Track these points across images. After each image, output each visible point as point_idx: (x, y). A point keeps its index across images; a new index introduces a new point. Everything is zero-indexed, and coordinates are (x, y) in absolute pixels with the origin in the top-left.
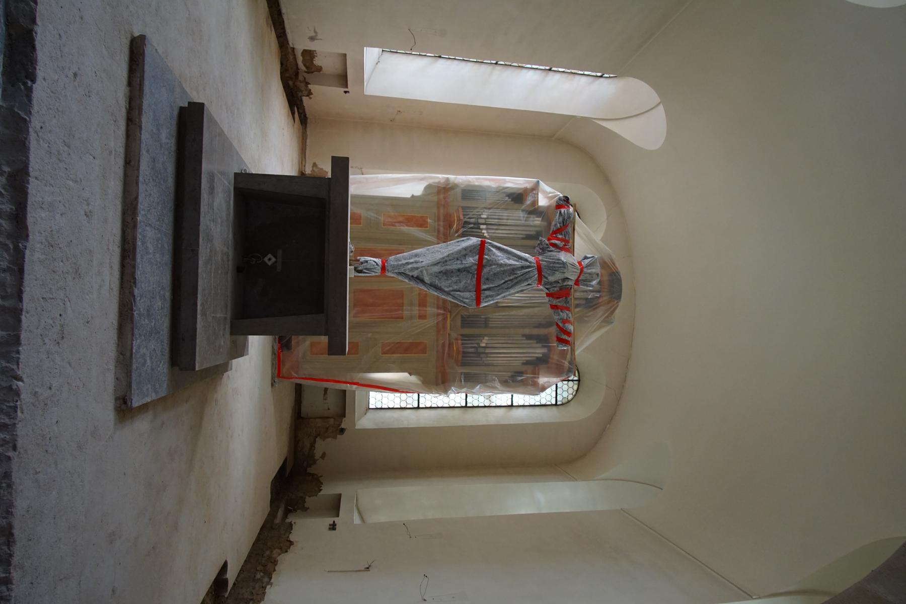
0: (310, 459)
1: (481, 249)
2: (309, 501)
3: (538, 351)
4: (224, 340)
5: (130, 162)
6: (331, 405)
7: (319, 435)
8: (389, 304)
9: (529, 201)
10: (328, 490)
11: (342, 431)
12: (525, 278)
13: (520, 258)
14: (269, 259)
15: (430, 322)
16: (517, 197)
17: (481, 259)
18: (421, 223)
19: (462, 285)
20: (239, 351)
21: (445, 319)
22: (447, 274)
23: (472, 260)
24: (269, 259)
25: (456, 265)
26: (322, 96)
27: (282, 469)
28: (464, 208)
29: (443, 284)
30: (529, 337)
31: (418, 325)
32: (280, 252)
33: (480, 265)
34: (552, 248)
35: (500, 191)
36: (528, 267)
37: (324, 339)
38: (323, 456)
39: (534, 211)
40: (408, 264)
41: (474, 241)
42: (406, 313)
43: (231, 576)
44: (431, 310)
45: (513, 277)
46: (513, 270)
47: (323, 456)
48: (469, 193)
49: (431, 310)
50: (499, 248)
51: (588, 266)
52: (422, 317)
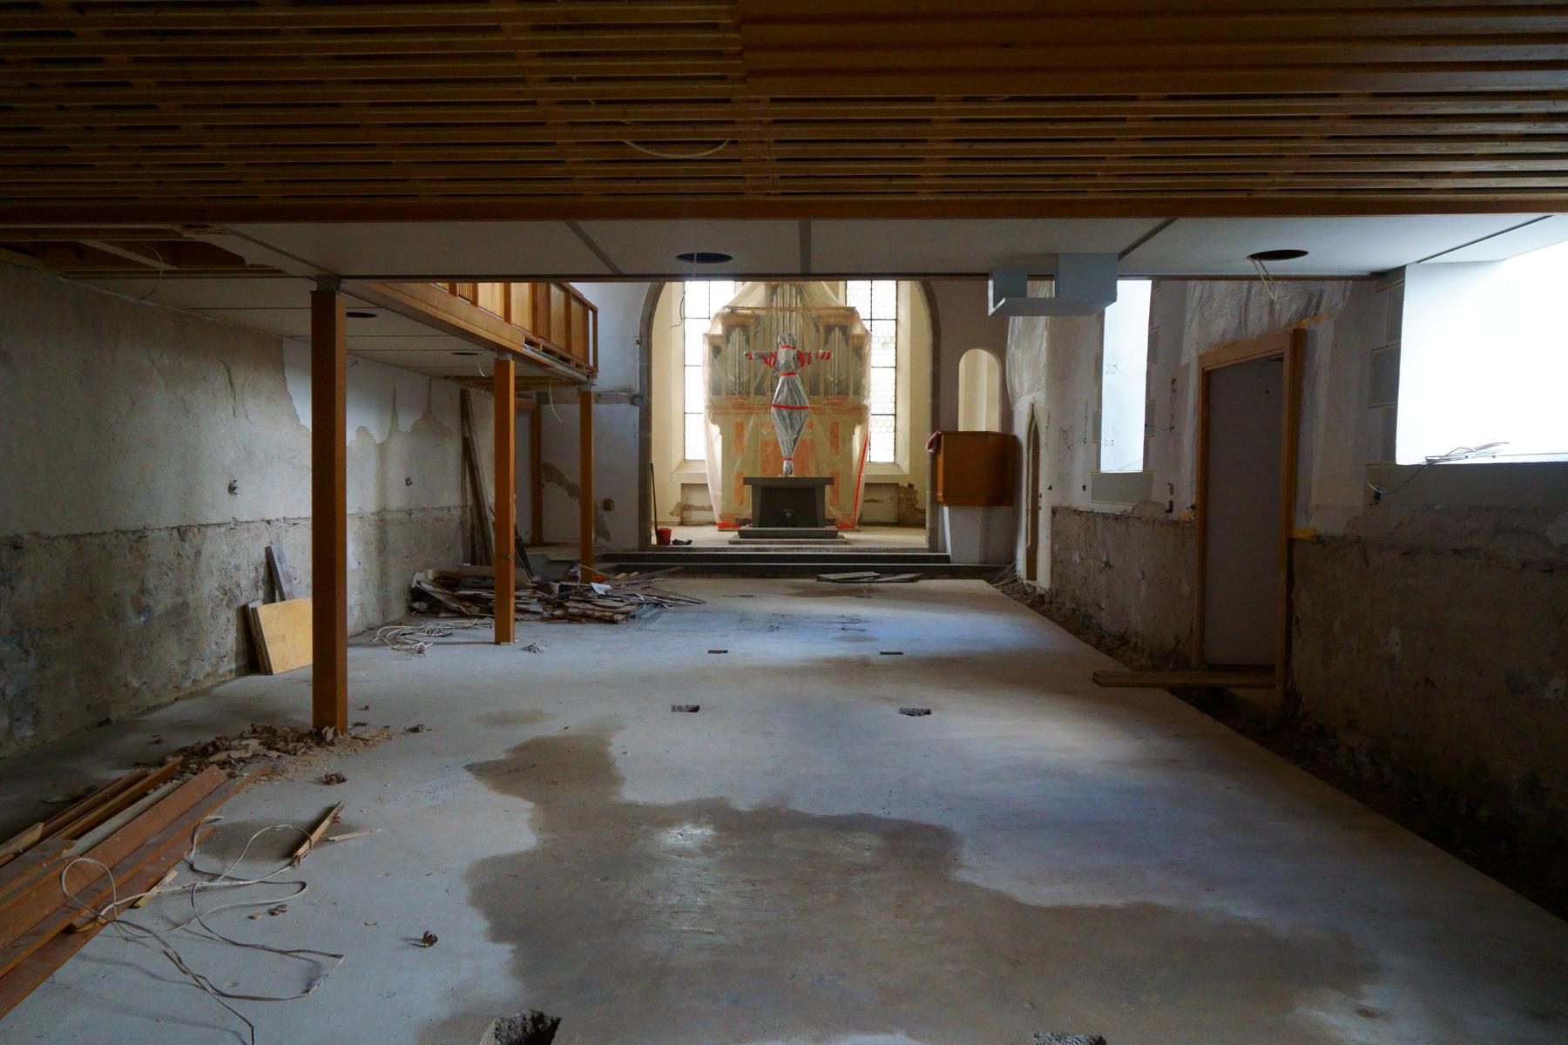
3: (837, 333)
6: (885, 496)
8: (802, 449)
14: (788, 515)
15: (815, 419)
18: (740, 428)
22: (792, 426)
23: (785, 412)
24: (788, 515)
30: (827, 342)
37: (827, 487)
39: (727, 336)
41: (773, 409)
45: (793, 389)
52: (811, 425)
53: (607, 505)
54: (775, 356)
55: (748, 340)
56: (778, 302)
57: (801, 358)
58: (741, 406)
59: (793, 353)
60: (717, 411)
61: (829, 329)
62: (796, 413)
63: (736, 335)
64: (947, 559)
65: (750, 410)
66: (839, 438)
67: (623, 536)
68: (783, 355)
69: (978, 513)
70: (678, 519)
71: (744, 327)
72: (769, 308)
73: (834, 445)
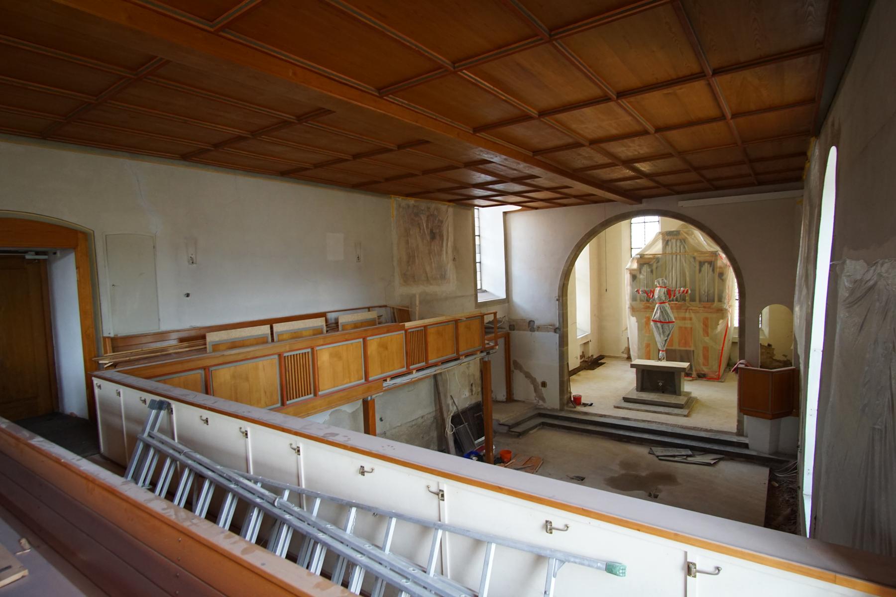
1: (654, 321)
4: (681, 397)
5: (638, 410)
7: (771, 357)
9: (634, 273)
11: (769, 345)
12: (664, 308)
14: (660, 384)
15: (693, 315)
16: (634, 277)
20: (688, 393)
22: (664, 332)
23: (659, 324)
24: (660, 384)
26: (593, 352)
29: (667, 333)
30: (700, 271)
31: (695, 320)
33: (660, 322)
35: (632, 286)
38: (785, 356)
41: (652, 323)
42: (689, 326)
44: (687, 315)
45: (663, 312)
46: (662, 312)
47: (785, 356)
48: (634, 299)
49: (687, 315)
52: (691, 319)
53: (544, 384)
55: (652, 271)
56: (669, 250)
57: (669, 293)
59: (663, 290)
60: (634, 310)
61: (701, 264)
62: (666, 325)
63: (646, 269)
64: (746, 446)
66: (707, 326)
67: (552, 399)
69: (768, 423)
70: (626, 356)
72: (664, 253)
73: (706, 333)
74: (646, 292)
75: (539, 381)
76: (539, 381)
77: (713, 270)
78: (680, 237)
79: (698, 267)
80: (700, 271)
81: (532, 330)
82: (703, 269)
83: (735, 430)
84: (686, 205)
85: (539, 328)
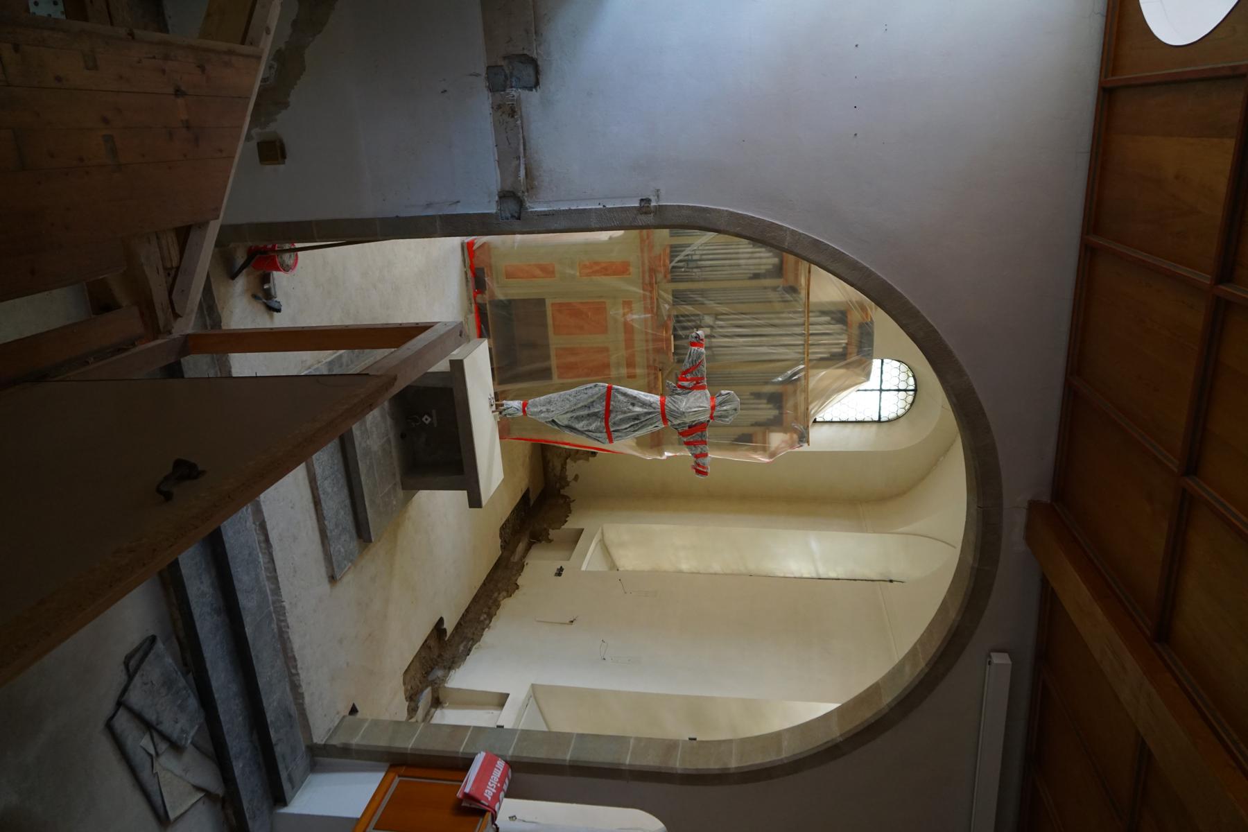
0: (563, 480)
2: (553, 533)
10: (572, 524)
13: (644, 404)
14: (427, 419)
17: (608, 405)
19: (593, 427)
21: (656, 378)
23: (599, 408)
24: (427, 419)
25: (586, 412)
27: (525, 497)
28: (672, 246)
29: (579, 426)
30: (758, 396)
32: (434, 412)
33: (608, 412)
34: (679, 390)
36: (650, 413)
37: (463, 495)
38: (576, 478)
40: (541, 412)
43: (449, 626)
46: (637, 418)
47: (576, 478)
50: (625, 394)
51: (721, 404)
54: (698, 386)
55: (756, 276)
56: (821, 325)
58: (653, 271)
59: (704, 418)
61: (776, 400)
65: (650, 286)
68: (694, 404)
71: (779, 271)
74: (696, 366)
75: (283, 125)
76: (283, 125)
77: (757, 424)
78: (853, 349)
79: (768, 389)
80: (758, 396)
81: (498, 80)
82: (763, 404)
83: (319, 738)
84: (995, 673)
85: (509, 113)
